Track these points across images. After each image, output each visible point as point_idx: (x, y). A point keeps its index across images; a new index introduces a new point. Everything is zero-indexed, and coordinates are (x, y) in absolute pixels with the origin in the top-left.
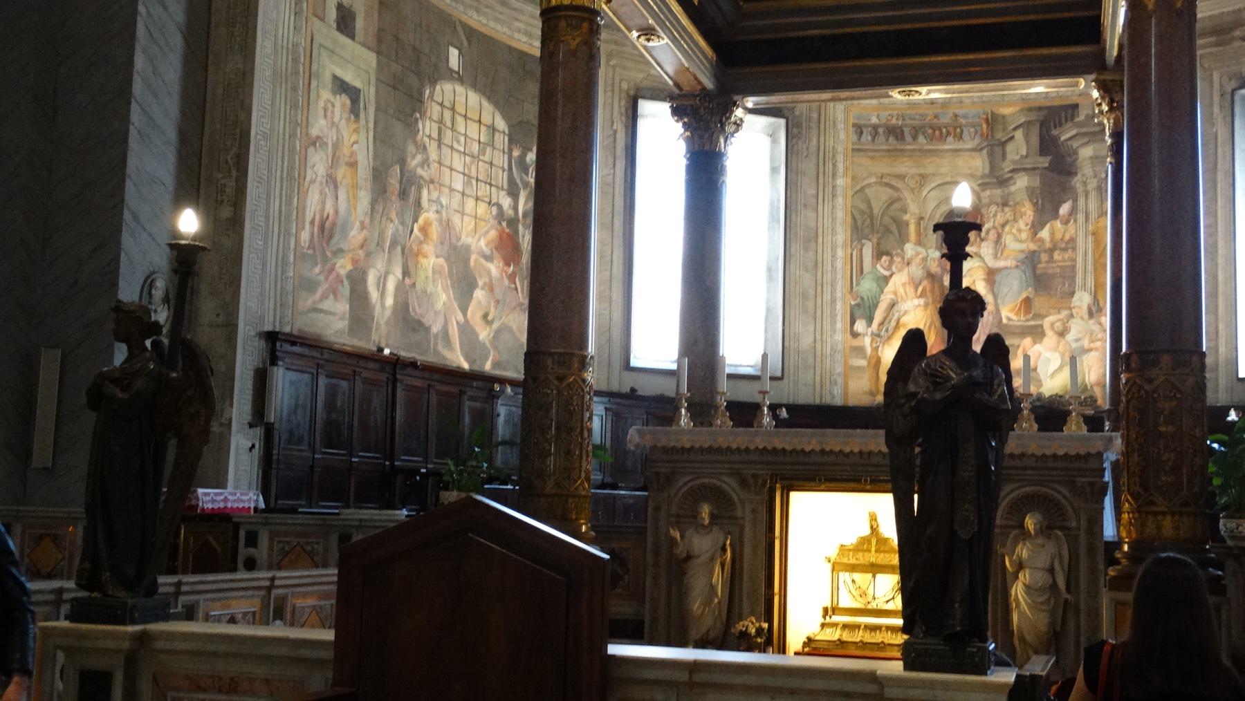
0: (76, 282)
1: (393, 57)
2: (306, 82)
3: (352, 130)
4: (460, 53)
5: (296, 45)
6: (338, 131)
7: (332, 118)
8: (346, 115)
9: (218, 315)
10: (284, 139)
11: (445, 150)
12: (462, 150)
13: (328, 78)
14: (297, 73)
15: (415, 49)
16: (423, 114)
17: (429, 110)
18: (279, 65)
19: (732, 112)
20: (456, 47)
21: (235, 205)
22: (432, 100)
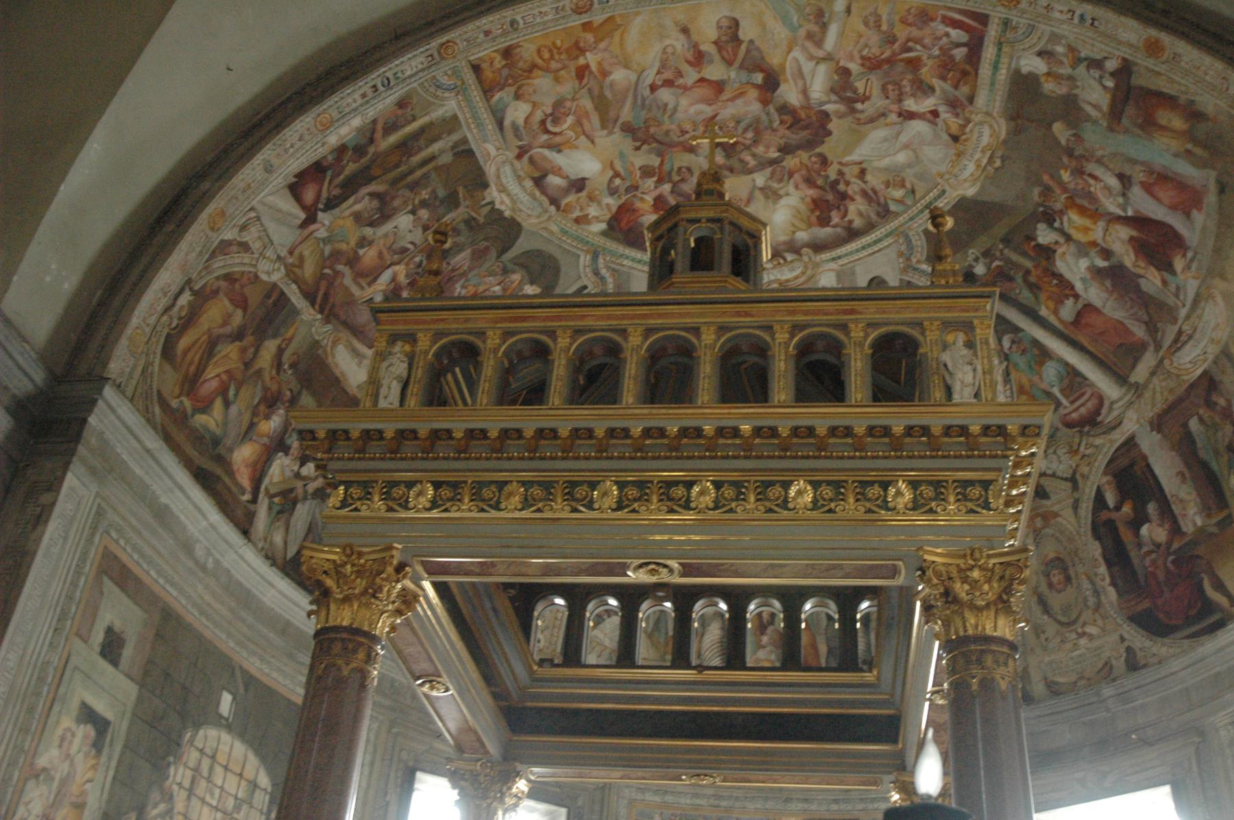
1: (157, 692)
2: (48, 704)
3: (88, 766)
4: (234, 699)
5: (47, 663)
6: (72, 764)
7: (69, 749)
8: (85, 749)
11: (195, 802)
12: (214, 803)
13: (75, 704)
14: (38, 694)
15: (184, 687)
16: (178, 758)
17: (186, 754)
19: (515, 782)
20: (230, 692)
22: (192, 745)
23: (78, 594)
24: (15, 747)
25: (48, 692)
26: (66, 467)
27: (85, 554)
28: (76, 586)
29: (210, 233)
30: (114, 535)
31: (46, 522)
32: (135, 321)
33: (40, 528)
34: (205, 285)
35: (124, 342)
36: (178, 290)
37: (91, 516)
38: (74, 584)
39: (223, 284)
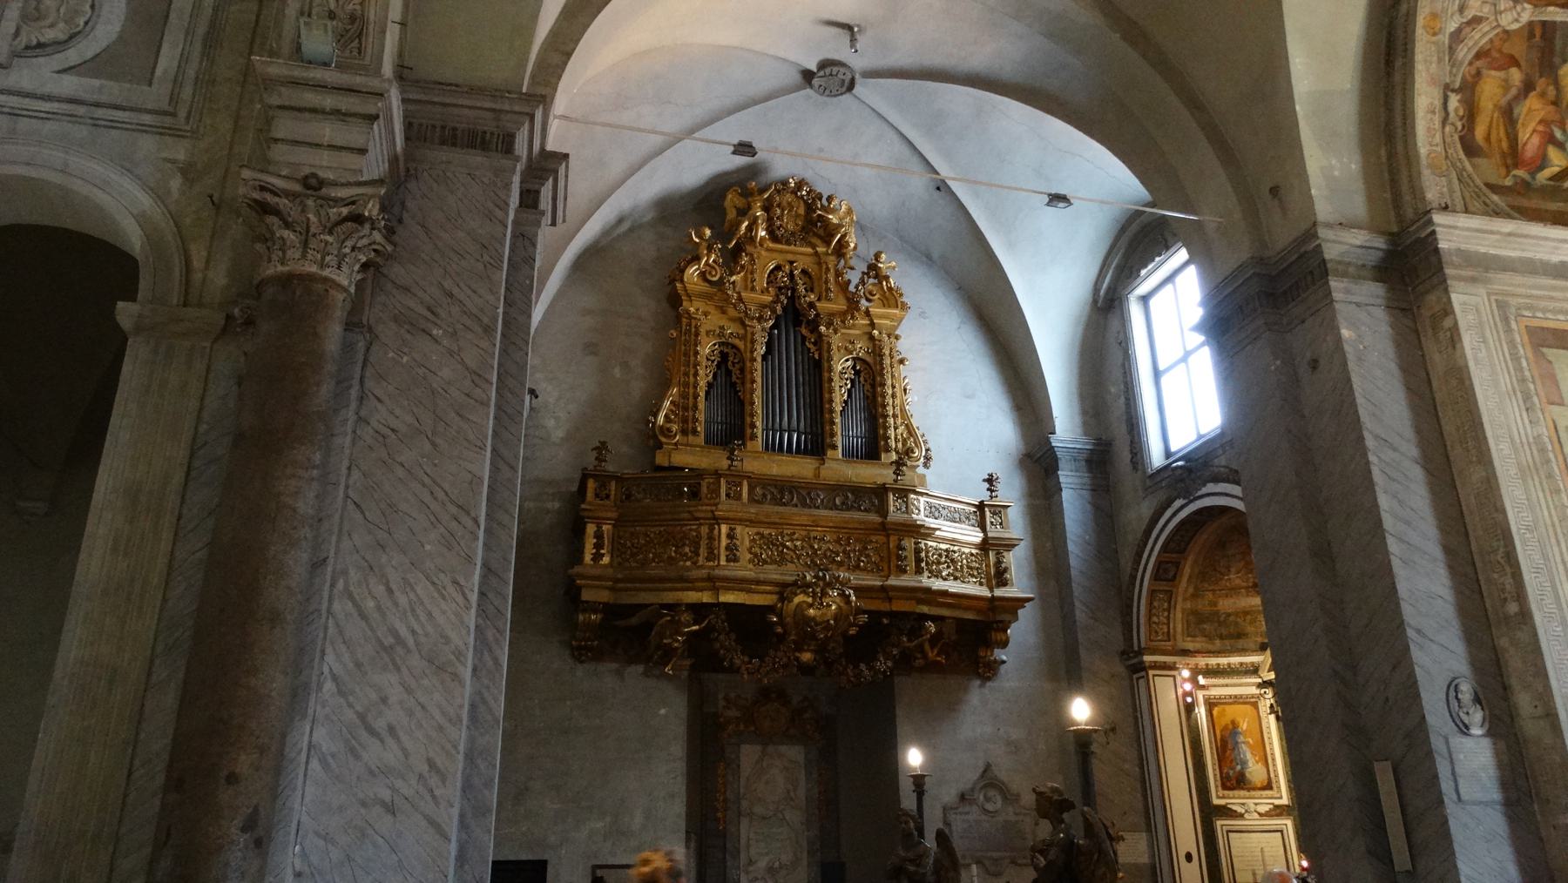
0: (1387, 699)
5: (1538, 438)
9: (1536, 707)
10: (1553, 525)
14: (1548, 461)
18: (1525, 463)
21: (1518, 600)
23: (1527, 373)
24: (1556, 508)
25: (1556, 457)
26: (1446, 291)
27: (1512, 344)
28: (1521, 370)
29: (1434, 39)
30: (1527, 313)
31: (1460, 339)
32: (1423, 150)
33: (1458, 346)
34: (1464, 76)
35: (1426, 173)
36: (1442, 101)
37: (1496, 312)
38: (1519, 369)
39: (1478, 63)
